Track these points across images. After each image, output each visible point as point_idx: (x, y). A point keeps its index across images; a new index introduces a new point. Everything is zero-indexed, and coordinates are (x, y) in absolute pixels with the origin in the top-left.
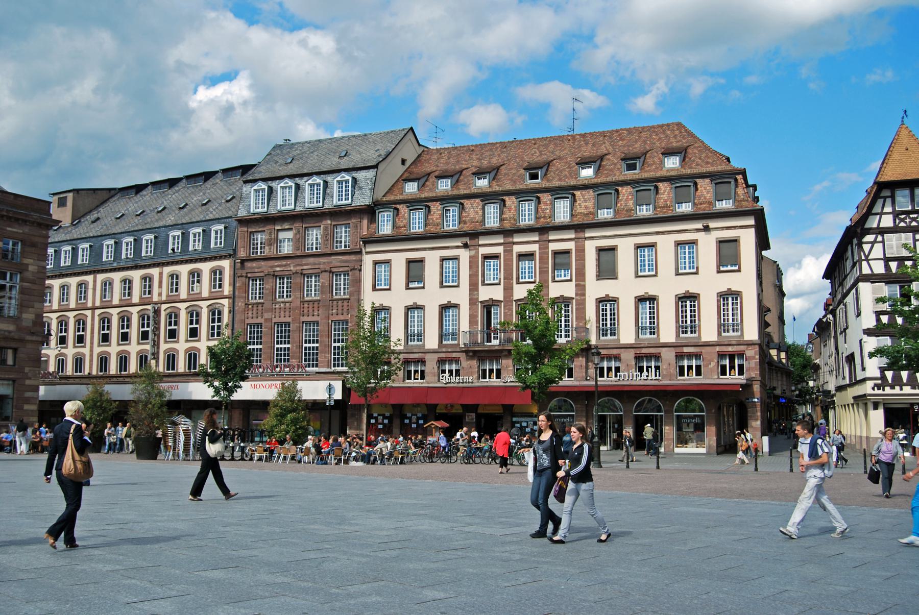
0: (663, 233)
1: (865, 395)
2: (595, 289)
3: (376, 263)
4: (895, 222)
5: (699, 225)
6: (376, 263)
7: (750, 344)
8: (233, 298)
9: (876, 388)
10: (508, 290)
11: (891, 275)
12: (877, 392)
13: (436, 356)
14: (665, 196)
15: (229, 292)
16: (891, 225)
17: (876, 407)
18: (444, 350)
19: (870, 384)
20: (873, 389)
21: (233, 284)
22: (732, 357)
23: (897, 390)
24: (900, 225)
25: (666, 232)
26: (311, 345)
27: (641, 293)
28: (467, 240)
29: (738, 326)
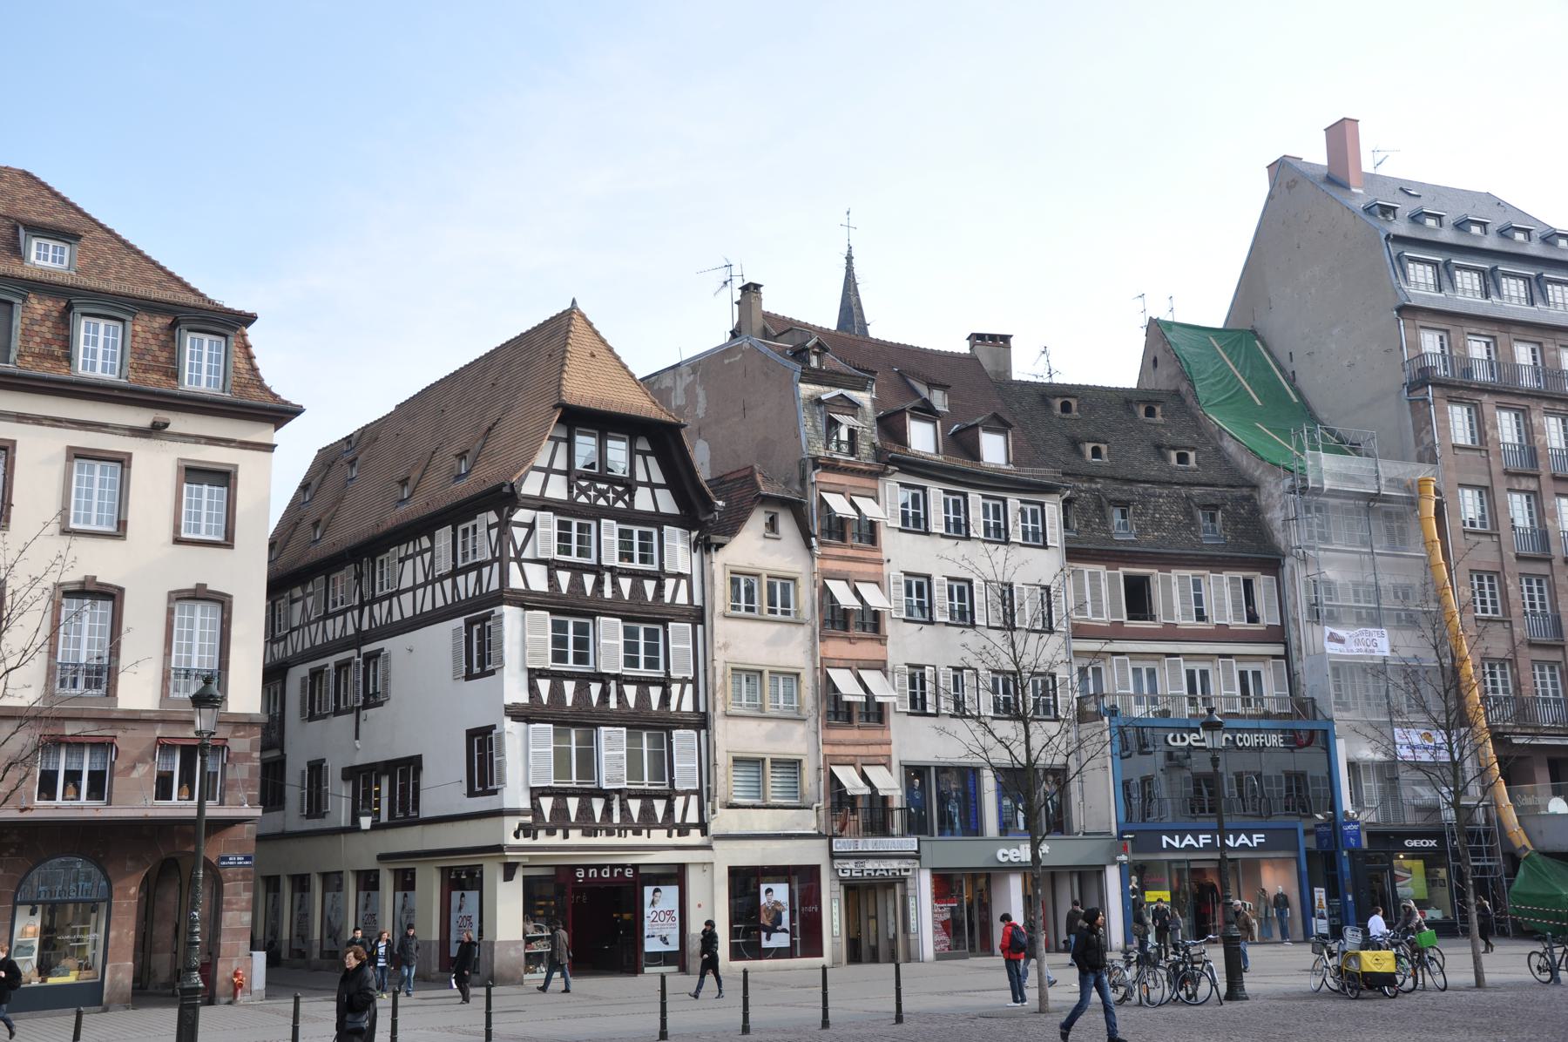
0: (38, 420)
1: (499, 848)
4: (570, 491)
7: (241, 723)
9: (521, 833)
11: (559, 598)
12: (523, 841)
14: (44, 329)
16: (563, 495)
17: (508, 876)
19: (512, 823)
20: (517, 835)
22: (188, 753)
23: (557, 839)
24: (578, 500)
25: (46, 418)
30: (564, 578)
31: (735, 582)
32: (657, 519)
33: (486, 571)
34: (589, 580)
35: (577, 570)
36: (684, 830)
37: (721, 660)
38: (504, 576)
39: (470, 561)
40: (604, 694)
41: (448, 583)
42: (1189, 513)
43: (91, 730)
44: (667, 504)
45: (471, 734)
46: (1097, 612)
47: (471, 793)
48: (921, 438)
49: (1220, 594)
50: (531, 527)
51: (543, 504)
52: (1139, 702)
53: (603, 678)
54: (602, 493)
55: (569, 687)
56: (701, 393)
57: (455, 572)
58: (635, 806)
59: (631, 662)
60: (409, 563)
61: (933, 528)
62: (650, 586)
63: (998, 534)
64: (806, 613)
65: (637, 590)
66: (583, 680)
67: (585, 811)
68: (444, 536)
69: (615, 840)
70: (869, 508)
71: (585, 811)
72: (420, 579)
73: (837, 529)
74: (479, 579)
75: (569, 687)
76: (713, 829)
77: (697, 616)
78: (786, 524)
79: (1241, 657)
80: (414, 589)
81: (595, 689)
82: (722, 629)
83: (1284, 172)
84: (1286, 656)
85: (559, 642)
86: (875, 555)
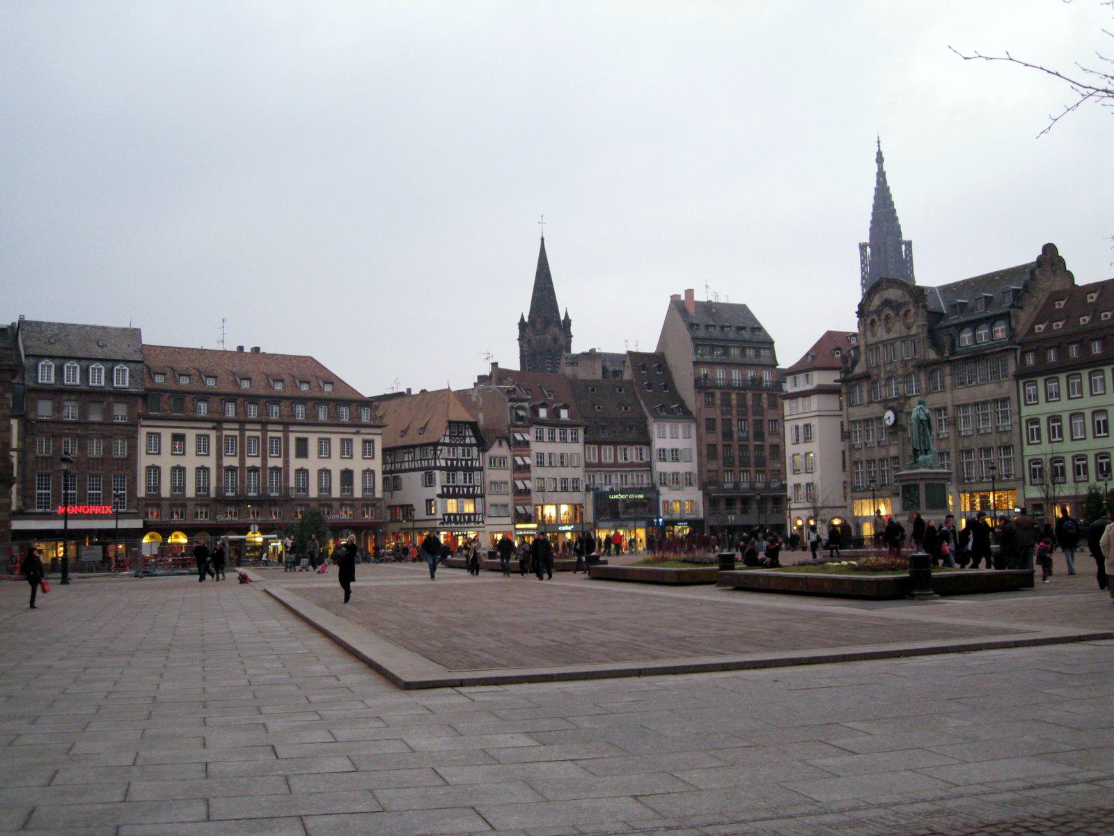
2: (295, 463)
3: (148, 433)
5: (354, 430)
6: (148, 433)
8: (22, 452)
10: (242, 460)
13: (194, 503)
15: (18, 446)
16: (449, 442)
18: (200, 498)
19: (439, 522)
21: (22, 438)
23: (449, 525)
26: (44, 492)
27: (321, 467)
28: (215, 424)
29: (373, 489)
30: (449, 462)
31: (491, 459)
32: (471, 445)
33: (430, 461)
34: (455, 462)
35: (452, 460)
36: (478, 523)
37: (487, 480)
38: (435, 463)
39: (425, 457)
40: (459, 490)
41: (419, 462)
42: (625, 429)
43: (349, 502)
44: (474, 441)
45: (427, 501)
46: (594, 459)
47: (427, 514)
48: (543, 413)
49: (632, 454)
50: (441, 450)
51: (444, 444)
52: (606, 484)
53: (459, 487)
54: (458, 440)
55: (451, 489)
56: (481, 399)
57: (421, 460)
58: (467, 517)
59: (465, 482)
60: (407, 455)
61: (545, 440)
62: (469, 463)
63: (564, 440)
64: (509, 466)
65: (467, 464)
66: (454, 487)
67: (455, 519)
68: (418, 451)
69: (462, 525)
70: (527, 437)
71: (455, 519)
72: (410, 459)
73: (518, 443)
74: (428, 463)
75: (451, 489)
76: (486, 523)
77: (481, 469)
78: (504, 444)
79: (637, 471)
80: (409, 461)
81: (457, 489)
82: (487, 472)
83: (675, 300)
84: (651, 470)
85: (448, 478)
86: (527, 449)
